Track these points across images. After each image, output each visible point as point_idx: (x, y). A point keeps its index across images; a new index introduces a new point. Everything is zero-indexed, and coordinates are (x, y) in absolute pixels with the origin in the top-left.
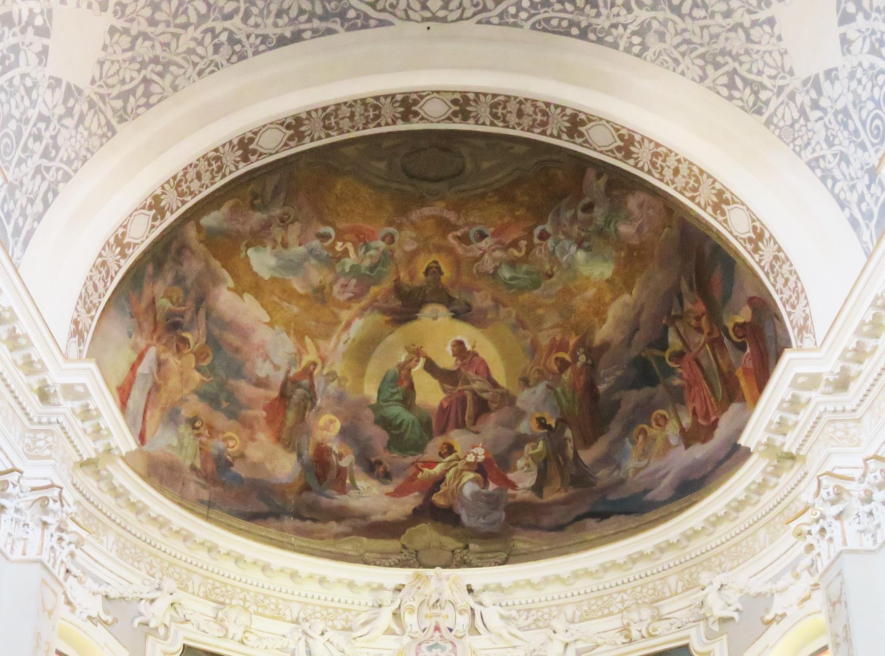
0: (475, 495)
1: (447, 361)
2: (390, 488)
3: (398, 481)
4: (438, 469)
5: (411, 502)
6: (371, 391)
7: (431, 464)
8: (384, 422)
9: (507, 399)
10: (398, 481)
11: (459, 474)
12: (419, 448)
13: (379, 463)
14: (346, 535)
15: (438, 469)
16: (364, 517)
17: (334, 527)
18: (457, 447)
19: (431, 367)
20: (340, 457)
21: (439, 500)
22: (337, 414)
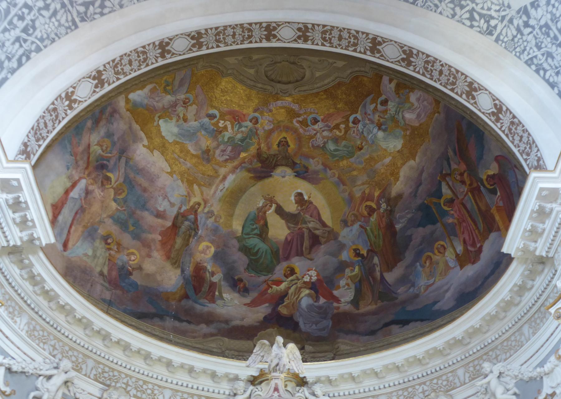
0: (310, 307)
1: (291, 207)
2: (248, 300)
3: (254, 295)
4: (283, 286)
5: (263, 311)
6: (237, 226)
7: (278, 283)
8: (246, 250)
9: (332, 235)
10: (254, 295)
11: (298, 291)
12: (270, 270)
13: (241, 280)
14: (212, 335)
15: (283, 286)
16: (227, 322)
17: (204, 328)
18: (297, 270)
19: (280, 211)
20: (213, 274)
21: (283, 310)
22: (212, 242)
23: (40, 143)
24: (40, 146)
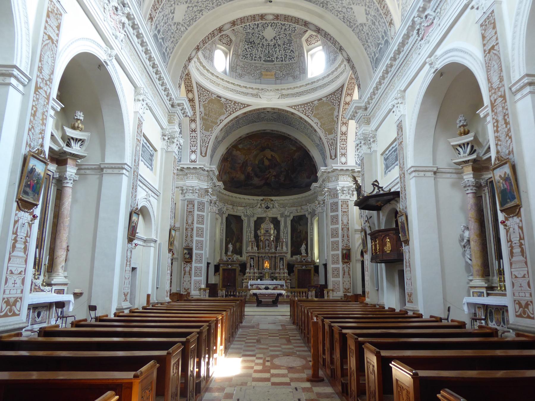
23: (156, 11)
24: (156, 13)
